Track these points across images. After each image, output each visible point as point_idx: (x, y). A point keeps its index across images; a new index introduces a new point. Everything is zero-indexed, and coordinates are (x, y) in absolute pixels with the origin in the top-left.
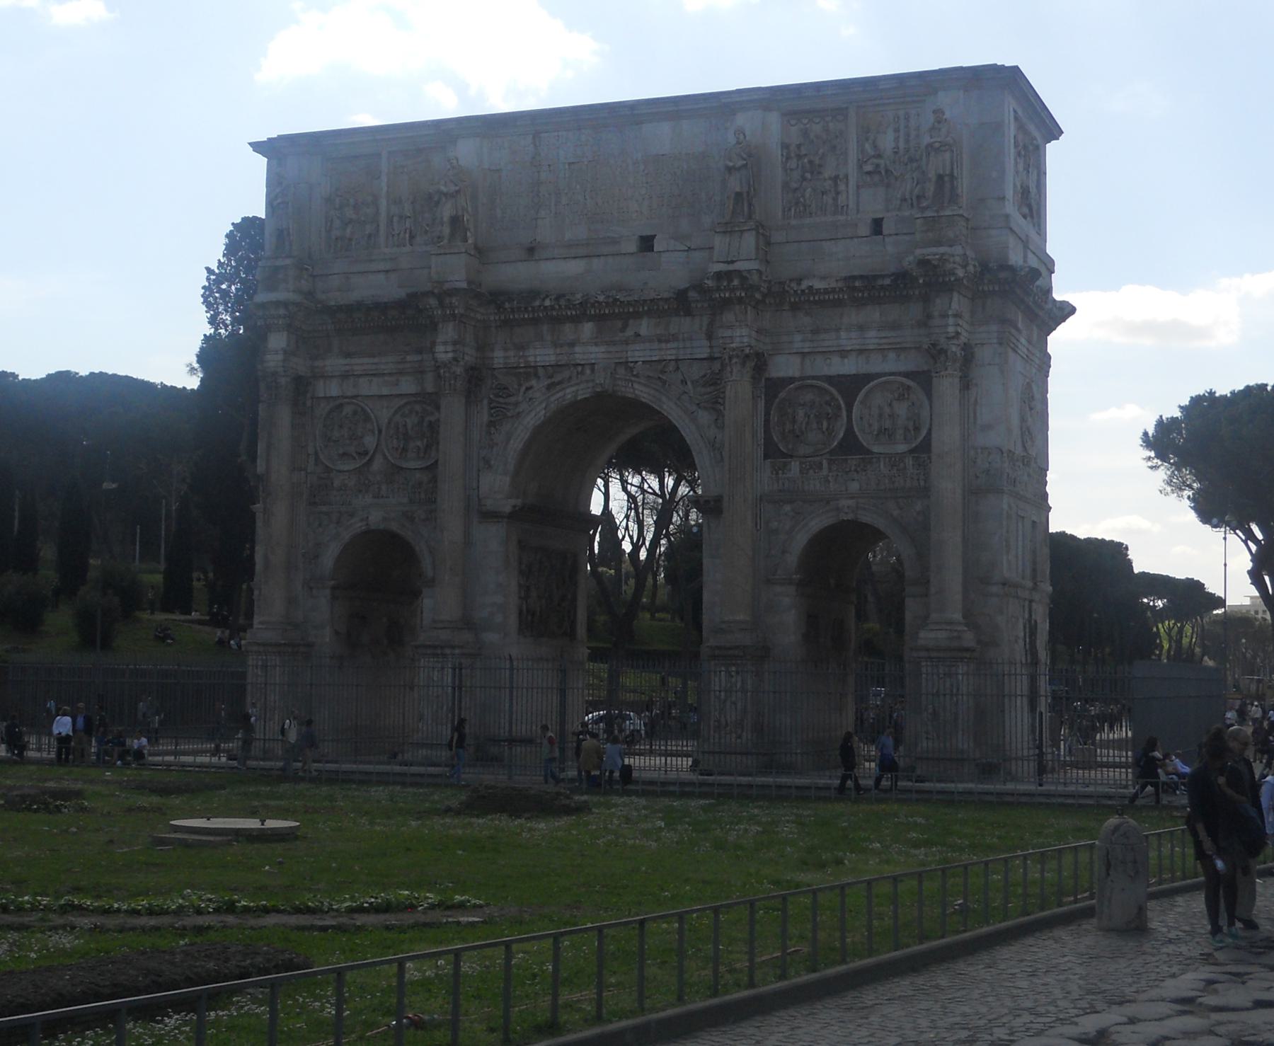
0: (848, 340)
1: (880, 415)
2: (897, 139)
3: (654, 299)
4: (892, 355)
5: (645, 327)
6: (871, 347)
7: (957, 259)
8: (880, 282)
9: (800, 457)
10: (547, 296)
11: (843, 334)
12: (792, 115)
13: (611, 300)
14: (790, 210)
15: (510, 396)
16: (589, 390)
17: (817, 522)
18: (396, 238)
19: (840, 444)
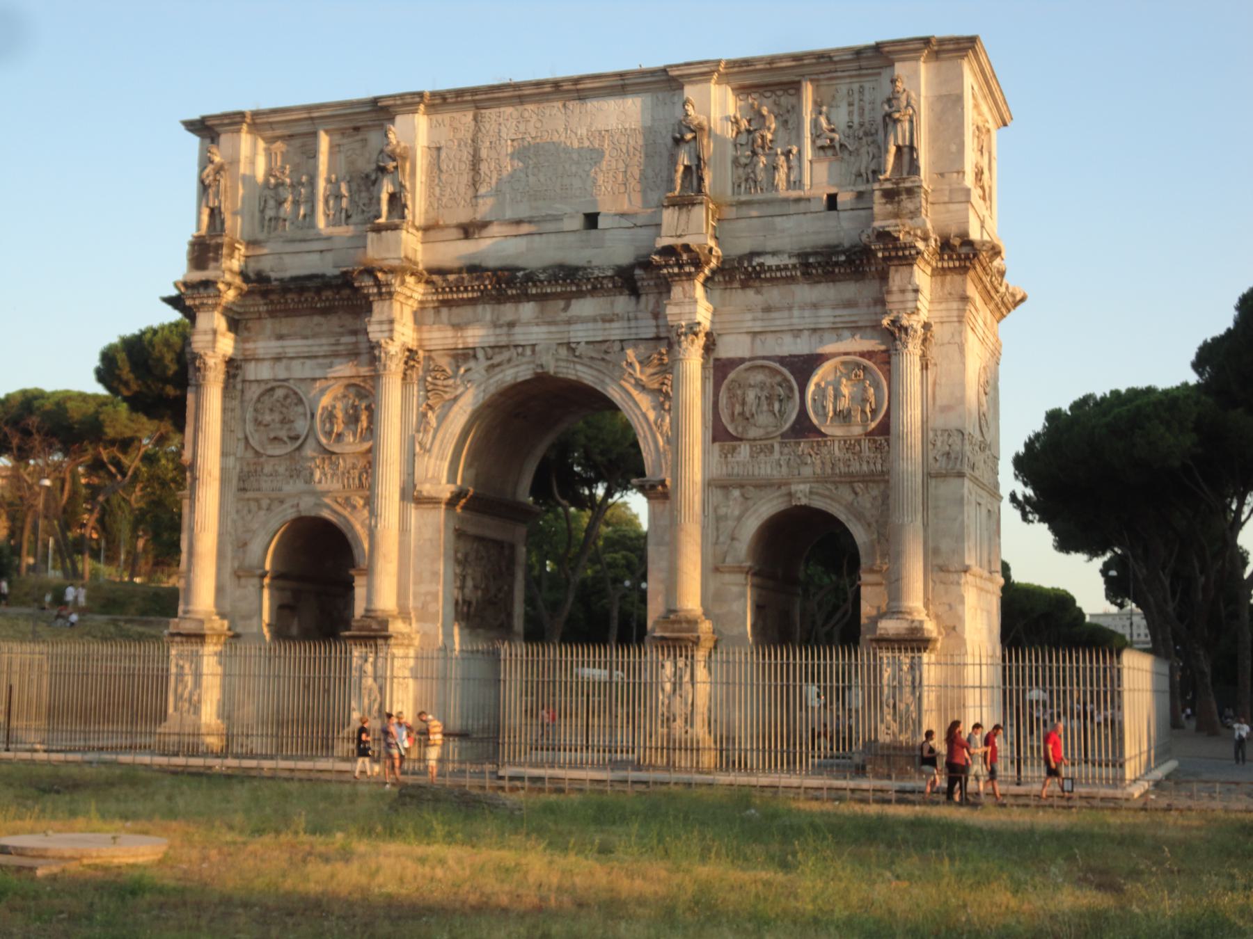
0: (800, 319)
2: (850, 113)
3: (597, 278)
5: (585, 307)
7: (919, 232)
8: (834, 259)
9: (749, 440)
11: (796, 313)
14: (739, 186)
17: (767, 507)
19: (793, 428)
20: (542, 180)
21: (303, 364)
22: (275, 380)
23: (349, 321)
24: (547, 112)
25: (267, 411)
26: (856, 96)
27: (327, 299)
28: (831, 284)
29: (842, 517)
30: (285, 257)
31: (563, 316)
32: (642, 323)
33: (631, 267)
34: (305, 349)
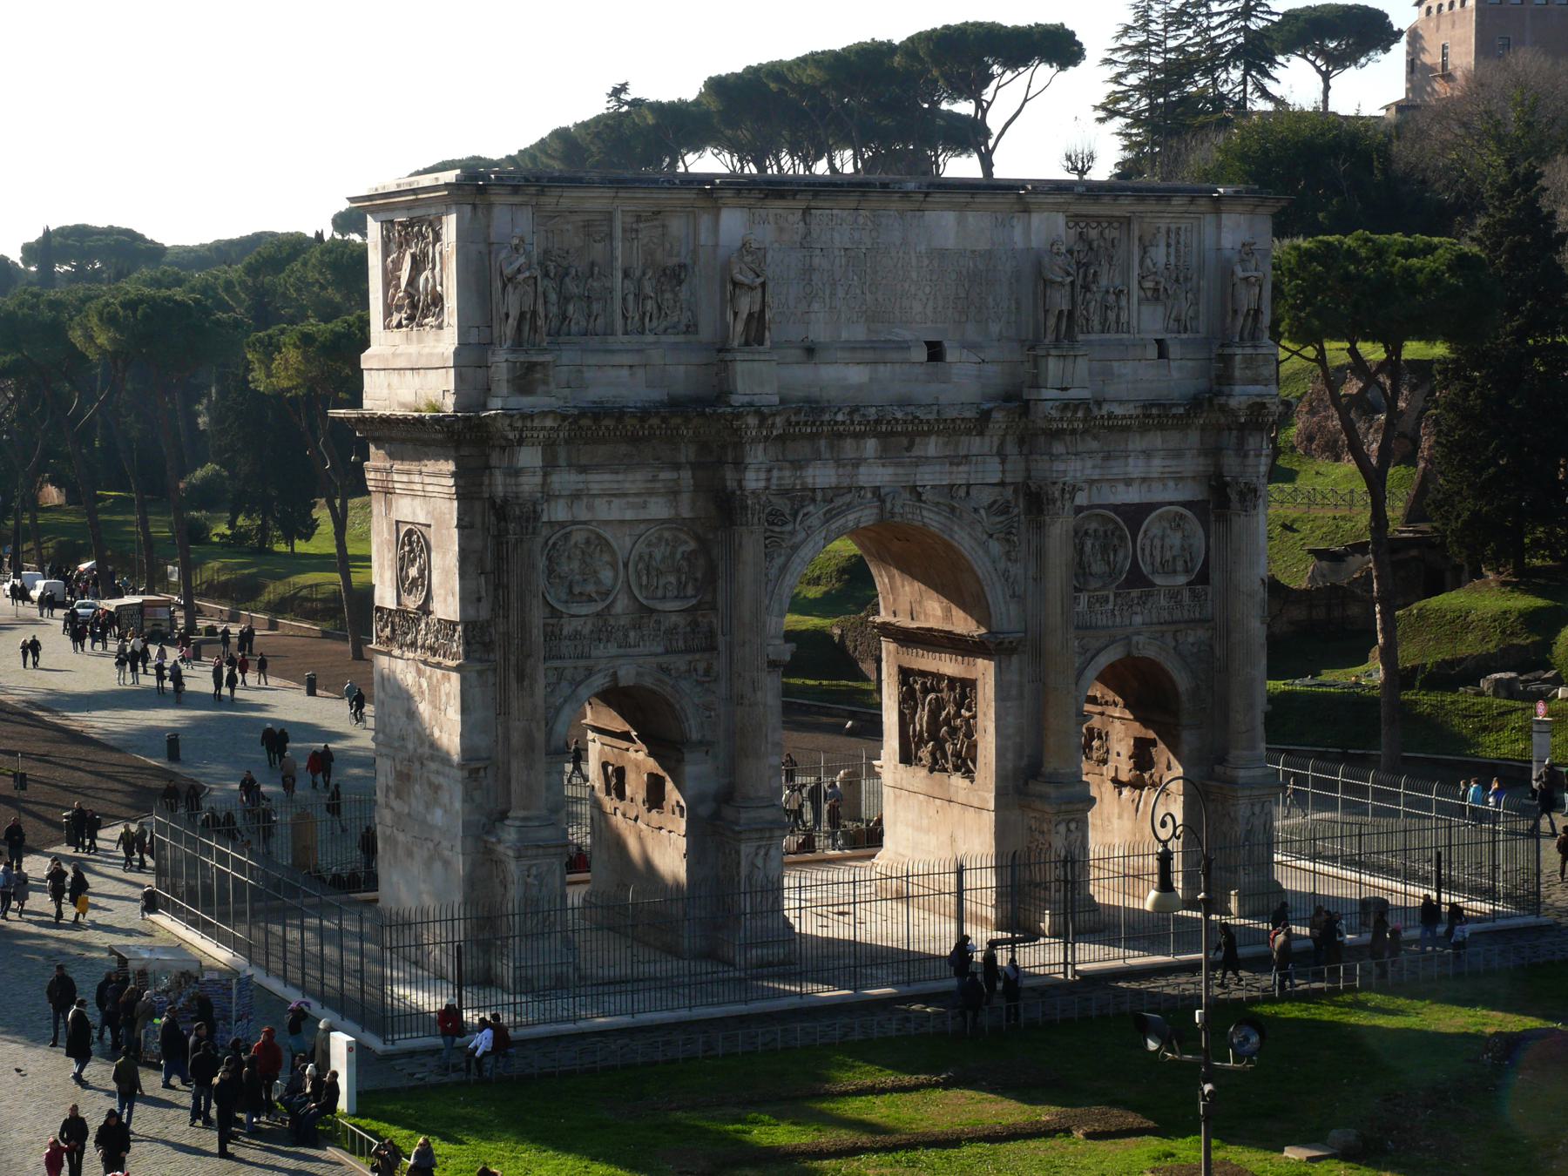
0: (1135, 468)
1: (1162, 547)
2: (1168, 255)
3: (953, 420)
4: (1171, 484)
5: (932, 447)
6: (1156, 475)
8: (1174, 411)
10: (840, 410)
11: (1131, 461)
12: (1074, 219)
13: (910, 417)
15: (785, 523)
16: (873, 517)
18: (629, 321)
20: (880, 300)
21: (610, 503)
22: (574, 523)
27: (651, 427)
28: (1159, 433)
29: (1169, 666)
30: (585, 369)
33: (990, 411)
34: (616, 486)
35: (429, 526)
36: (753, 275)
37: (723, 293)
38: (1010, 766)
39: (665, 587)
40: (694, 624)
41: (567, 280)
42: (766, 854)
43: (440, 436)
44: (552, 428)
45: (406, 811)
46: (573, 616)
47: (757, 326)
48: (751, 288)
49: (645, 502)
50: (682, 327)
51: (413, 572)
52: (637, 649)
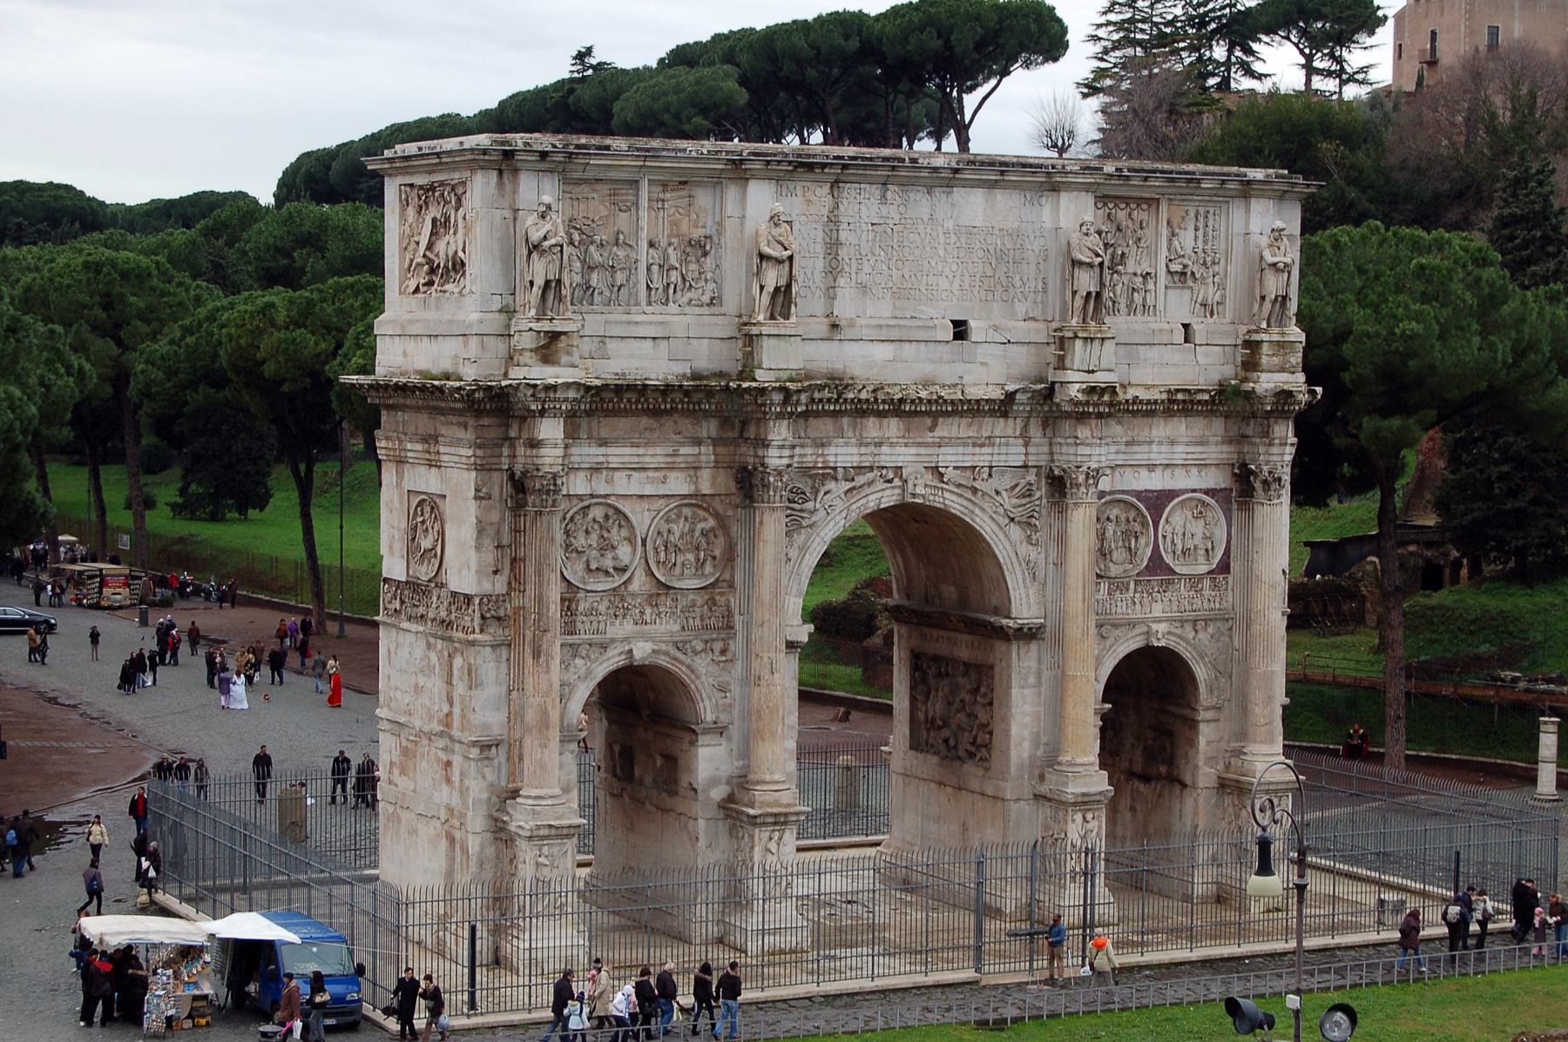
0: (1158, 454)
2: (1196, 237)
3: (978, 401)
4: (1194, 471)
8: (1200, 397)
11: (1155, 448)
12: (1103, 199)
20: (907, 276)
21: (629, 477)
22: (592, 496)
23: (686, 425)
24: (912, 196)
25: (581, 535)
26: (1201, 219)
27: (673, 401)
29: (1187, 655)
31: (929, 437)
32: (1012, 450)
33: (1016, 391)
34: (636, 459)
35: (444, 496)
36: (781, 248)
37: (749, 266)
38: (1026, 755)
39: (683, 565)
40: (712, 602)
41: (592, 248)
42: (780, 839)
43: (459, 405)
44: (575, 400)
45: (412, 788)
46: (588, 591)
47: (782, 300)
48: (779, 261)
49: (665, 477)
50: (706, 299)
51: (426, 543)
52: (653, 627)
